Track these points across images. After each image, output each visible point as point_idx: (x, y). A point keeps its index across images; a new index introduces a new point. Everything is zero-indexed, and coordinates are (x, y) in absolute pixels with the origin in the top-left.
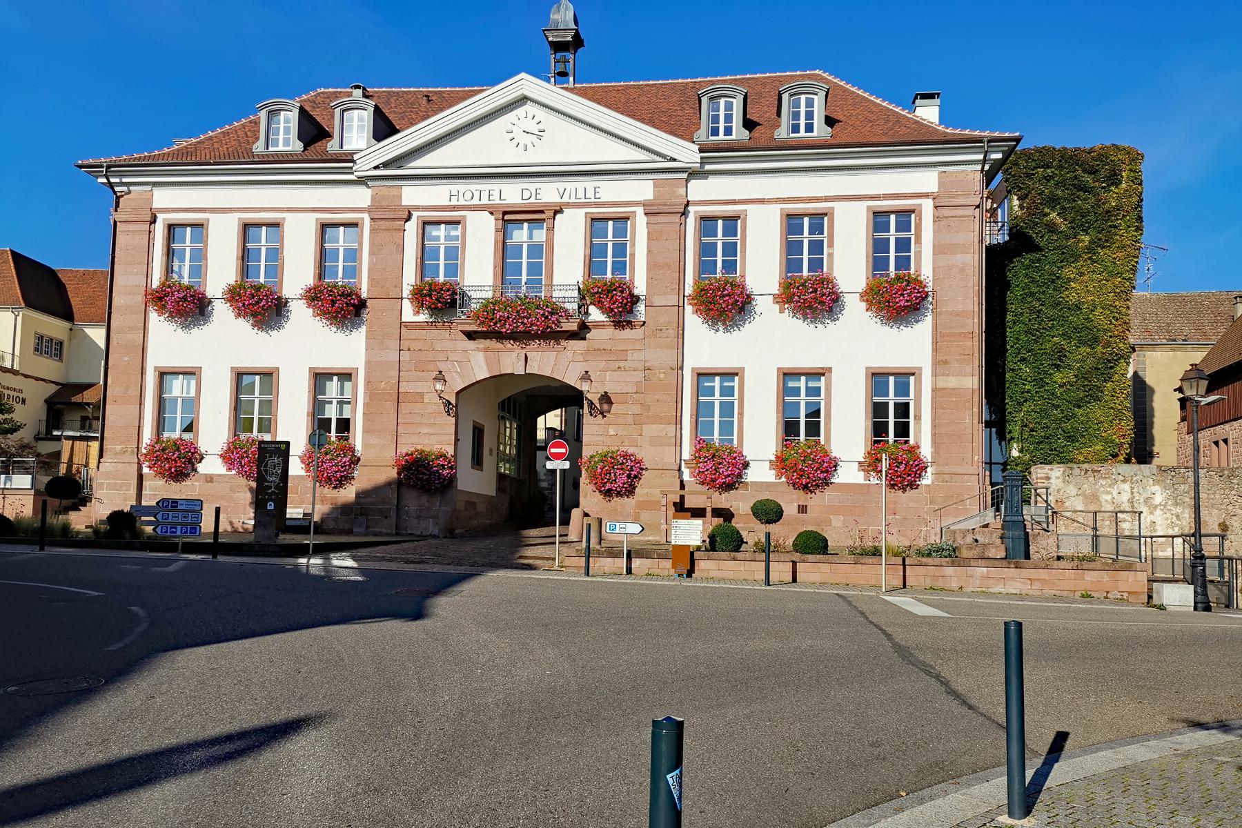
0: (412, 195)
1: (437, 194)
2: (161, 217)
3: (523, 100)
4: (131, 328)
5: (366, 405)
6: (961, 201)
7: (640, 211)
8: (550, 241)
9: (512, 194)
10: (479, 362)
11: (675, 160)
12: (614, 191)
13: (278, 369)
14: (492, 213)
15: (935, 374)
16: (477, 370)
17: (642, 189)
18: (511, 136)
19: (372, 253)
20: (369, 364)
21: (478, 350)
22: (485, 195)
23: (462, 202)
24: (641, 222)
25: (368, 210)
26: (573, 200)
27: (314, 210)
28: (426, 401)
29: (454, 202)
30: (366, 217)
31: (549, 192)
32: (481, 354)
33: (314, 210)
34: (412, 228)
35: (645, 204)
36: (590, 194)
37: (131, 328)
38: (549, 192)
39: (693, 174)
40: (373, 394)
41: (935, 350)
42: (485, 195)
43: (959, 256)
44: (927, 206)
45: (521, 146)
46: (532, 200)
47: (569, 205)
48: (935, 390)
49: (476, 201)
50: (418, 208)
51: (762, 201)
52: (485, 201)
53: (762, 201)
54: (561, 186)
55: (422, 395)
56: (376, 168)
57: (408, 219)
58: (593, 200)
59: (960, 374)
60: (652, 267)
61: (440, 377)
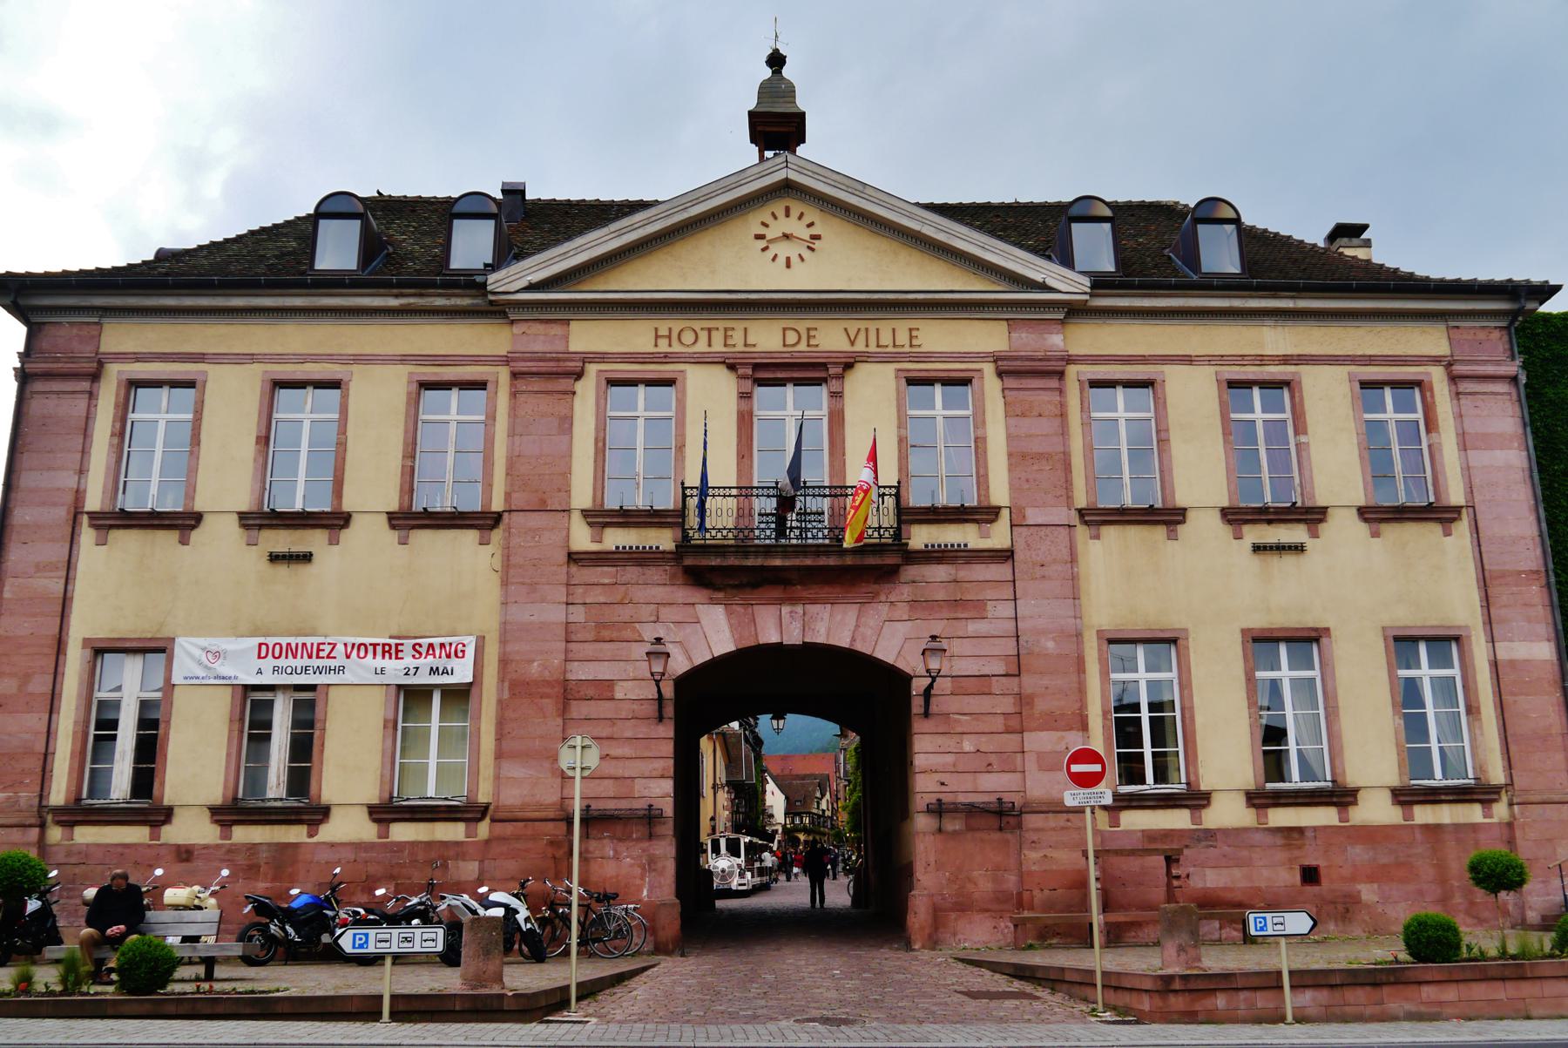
0: (586, 336)
1: (637, 336)
2: (115, 373)
4: (40, 568)
6: (1490, 369)
7: (988, 369)
9: (767, 337)
10: (711, 631)
14: (732, 367)
15: (1492, 640)
16: (713, 638)
17: (987, 337)
19: (512, 434)
21: (712, 602)
22: (718, 338)
23: (676, 348)
25: (506, 360)
26: (873, 348)
27: (404, 359)
28: (618, 695)
29: (663, 346)
30: (504, 374)
31: (831, 337)
32: (720, 609)
33: (404, 359)
34: (587, 389)
35: (996, 358)
36: (903, 338)
37: (40, 568)
38: (831, 337)
39: (1075, 311)
42: (718, 338)
43: (1498, 453)
45: (781, 260)
46: (803, 347)
48: (1495, 665)
49: (702, 346)
50: (602, 357)
51: (1187, 360)
52: (718, 346)
53: (1187, 360)
54: (853, 326)
55: (610, 684)
56: (531, 287)
57: (579, 375)
58: (907, 349)
59: (1529, 637)
61: (658, 652)
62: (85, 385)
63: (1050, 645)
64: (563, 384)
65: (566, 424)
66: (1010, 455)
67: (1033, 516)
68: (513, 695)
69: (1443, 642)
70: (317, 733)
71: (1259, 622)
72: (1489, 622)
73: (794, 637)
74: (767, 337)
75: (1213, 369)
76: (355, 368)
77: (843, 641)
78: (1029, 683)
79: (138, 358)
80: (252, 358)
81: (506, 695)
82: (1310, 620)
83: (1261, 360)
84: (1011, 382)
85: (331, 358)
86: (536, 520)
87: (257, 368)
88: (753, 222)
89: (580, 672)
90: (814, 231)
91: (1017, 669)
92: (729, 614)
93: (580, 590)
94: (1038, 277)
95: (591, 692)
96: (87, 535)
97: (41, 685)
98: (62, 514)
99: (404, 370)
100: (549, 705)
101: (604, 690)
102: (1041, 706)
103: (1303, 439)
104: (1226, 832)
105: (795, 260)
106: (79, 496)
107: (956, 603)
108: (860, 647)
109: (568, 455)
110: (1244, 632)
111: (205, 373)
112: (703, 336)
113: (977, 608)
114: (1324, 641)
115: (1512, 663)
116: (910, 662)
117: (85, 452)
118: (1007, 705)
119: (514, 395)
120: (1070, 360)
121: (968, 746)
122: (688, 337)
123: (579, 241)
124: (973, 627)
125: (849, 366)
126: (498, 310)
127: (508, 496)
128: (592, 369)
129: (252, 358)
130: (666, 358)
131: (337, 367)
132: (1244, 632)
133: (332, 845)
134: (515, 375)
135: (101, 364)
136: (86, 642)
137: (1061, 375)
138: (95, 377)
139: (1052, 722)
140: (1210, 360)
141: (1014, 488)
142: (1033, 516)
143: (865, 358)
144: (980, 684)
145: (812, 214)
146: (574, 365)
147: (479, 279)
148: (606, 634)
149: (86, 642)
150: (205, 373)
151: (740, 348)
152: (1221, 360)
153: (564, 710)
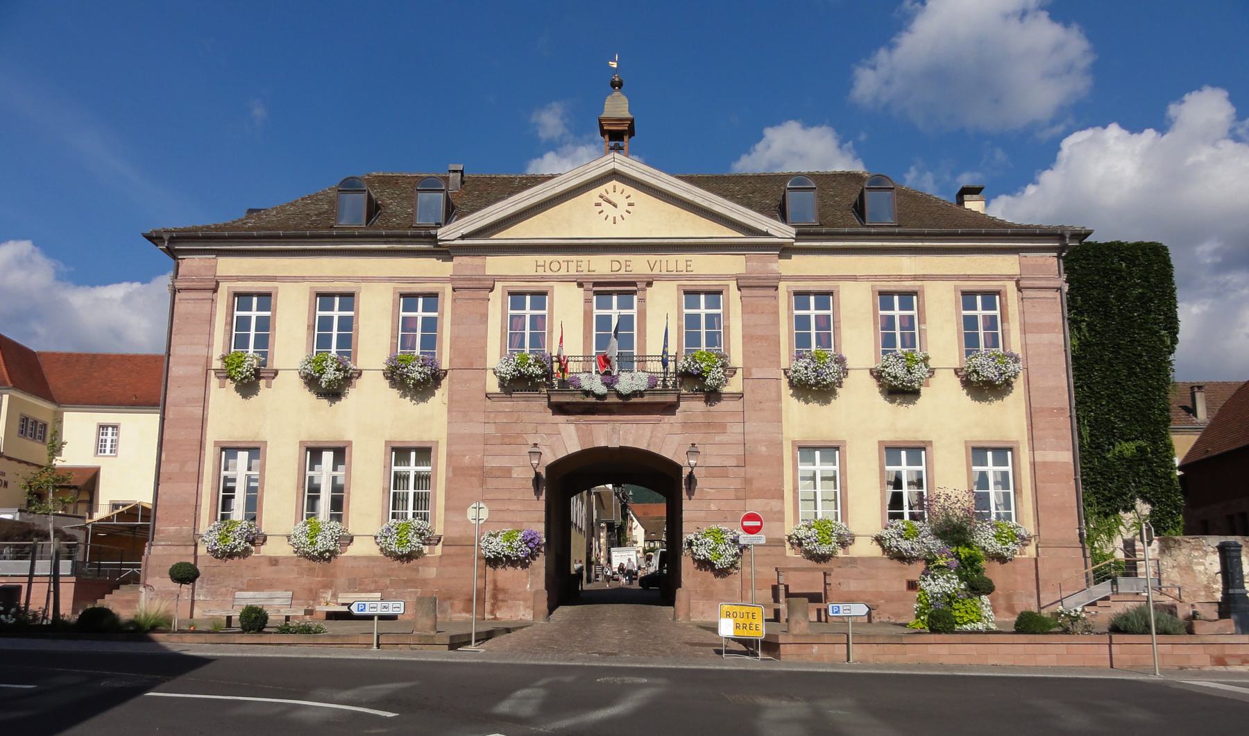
0: (495, 265)
2: (224, 287)
3: (615, 175)
4: (189, 401)
5: (449, 480)
7: (733, 285)
8: (642, 314)
9: (602, 265)
10: (569, 438)
11: (767, 234)
12: (703, 264)
13: (350, 443)
14: (580, 285)
17: (733, 264)
18: (599, 209)
20: (451, 440)
23: (549, 273)
24: (733, 295)
25: (452, 279)
26: (664, 272)
28: (514, 475)
29: (541, 272)
30: (448, 288)
32: (572, 427)
33: (391, 279)
36: (682, 266)
37: (189, 401)
38: (639, 264)
39: (785, 251)
40: (456, 471)
41: (1031, 426)
44: (1011, 287)
46: (622, 272)
47: (660, 278)
48: (1033, 464)
49: (563, 272)
51: (854, 278)
52: (573, 272)
53: (854, 278)
56: (463, 237)
57: (492, 290)
59: (1058, 448)
60: (747, 338)
62: (209, 295)
63: (764, 449)
64: (483, 293)
65: (484, 318)
66: (744, 337)
67: (756, 373)
68: (455, 475)
69: (1001, 452)
70: (345, 495)
71: (889, 437)
72: (1032, 439)
73: (615, 443)
74: (602, 265)
75: (870, 284)
76: (363, 285)
77: (643, 446)
78: (751, 471)
79: (239, 279)
80: (303, 279)
81: (451, 475)
82: (922, 437)
83: (901, 278)
84: (745, 292)
85: (348, 279)
86: (468, 374)
87: (307, 285)
88: (594, 194)
89: (492, 462)
90: (630, 201)
91: (743, 462)
92: (577, 430)
93: (492, 415)
94: (764, 229)
95: (498, 474)
96: (214, 382)
97: (192, 467)
98: (200, 370)
99: (391, 285)
100: (475, 480)
101: (506, 472)
102: (756, 485)
103: (923, 327)
104: (862, 559)
105: (618, 218)
106: (208, 360)
107: (709, 425)
108: (652, 449)
109: (485, 337)
110: (880, 443)
111: (276, 288)
112: (564, 265)
113: (722, 428)
114: (928, 449)
115: (1044, 464)
116: (680, 459)
117: (211, 334)
118: (737, 483)
119: (454, 300)
120: (780, 278)
121: (713, 507)
122: (555, 266)
123: (491, 208)
124: (718, 438)
125: (649, 284)
126: (446, 253)
127: (451, 360)
128: (499, 285)
129: (303, 279)
130: (543, 279)
131: (352, 284)
132: (880, 443)
133: (355, 558)
134: (454, 290)
135: (218, 283)
136: (216, 443)
137: (777, 288)
138: (215, 290)
139: (763, 494)
140: (868, 278)
141: (745, 356)
142: (756, 373)
143: (660, 278)
144: (722, 472)
145: (630, 190)
146: (489, 284)
147: (433, 232)
148: (506, 440)
149: (216, 443)
150: (276, 288)
151: (586, 272)
152: (875, 278)
153: (482, 484)
